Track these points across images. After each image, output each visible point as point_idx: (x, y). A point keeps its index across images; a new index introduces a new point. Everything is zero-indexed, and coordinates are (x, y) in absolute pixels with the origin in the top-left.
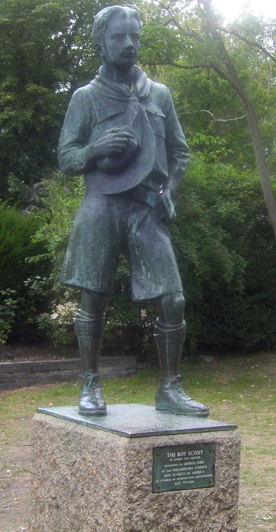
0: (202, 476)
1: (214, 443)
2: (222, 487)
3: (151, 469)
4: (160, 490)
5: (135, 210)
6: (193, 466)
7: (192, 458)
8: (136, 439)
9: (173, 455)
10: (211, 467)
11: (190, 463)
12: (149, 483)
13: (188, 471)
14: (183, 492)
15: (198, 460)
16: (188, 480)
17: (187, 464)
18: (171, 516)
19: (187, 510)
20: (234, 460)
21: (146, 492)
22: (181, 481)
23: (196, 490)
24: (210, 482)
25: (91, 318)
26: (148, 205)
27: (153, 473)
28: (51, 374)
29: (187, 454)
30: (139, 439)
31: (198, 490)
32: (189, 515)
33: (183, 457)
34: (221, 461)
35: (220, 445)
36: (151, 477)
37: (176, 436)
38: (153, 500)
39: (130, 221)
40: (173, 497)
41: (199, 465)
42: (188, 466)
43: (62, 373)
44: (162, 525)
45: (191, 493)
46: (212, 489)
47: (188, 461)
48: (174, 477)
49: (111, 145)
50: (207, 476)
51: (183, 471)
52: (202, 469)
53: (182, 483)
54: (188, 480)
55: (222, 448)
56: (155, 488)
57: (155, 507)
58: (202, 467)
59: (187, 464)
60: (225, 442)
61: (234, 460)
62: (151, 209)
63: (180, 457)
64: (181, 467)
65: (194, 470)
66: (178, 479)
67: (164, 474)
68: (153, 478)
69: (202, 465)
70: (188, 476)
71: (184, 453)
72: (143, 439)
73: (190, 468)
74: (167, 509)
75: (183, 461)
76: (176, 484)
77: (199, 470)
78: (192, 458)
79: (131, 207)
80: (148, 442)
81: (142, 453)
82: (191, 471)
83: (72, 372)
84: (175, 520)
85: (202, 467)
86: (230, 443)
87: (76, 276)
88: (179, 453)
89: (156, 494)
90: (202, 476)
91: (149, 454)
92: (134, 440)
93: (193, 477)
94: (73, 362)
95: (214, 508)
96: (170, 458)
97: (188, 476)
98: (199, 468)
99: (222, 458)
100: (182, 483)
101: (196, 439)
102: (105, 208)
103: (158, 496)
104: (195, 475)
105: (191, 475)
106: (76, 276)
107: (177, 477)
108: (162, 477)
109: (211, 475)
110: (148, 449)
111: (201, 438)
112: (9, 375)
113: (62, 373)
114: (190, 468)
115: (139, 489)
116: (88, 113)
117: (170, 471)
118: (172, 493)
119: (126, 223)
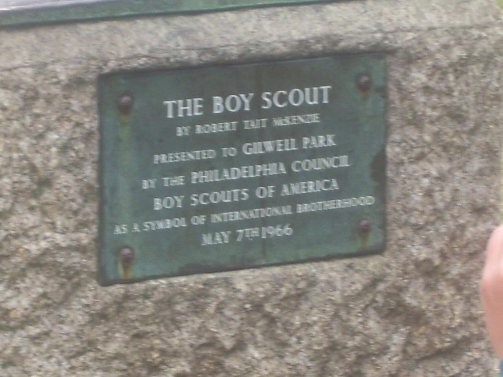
0: (330, 205)
3: (89, 172)
4: (136, 271)
6: (285, 158)
7: (278, 122)
9: (193, 107)
11: (269, 146)
12: (85, 237)
13: (264, 181)
14: (242, 280)
16: (264, 222)
22: (231, 227)
23: (299, 270)
24: (364, 231)
27: (100, 194)
29: (257, 102)
31: (311, 268)
33: (241, 116)
36: (90, 210)
37: (203, 19)
40: (197, 301)
41: (314, 153)
42: (263, 159)
45: (278, 282)
47: (261, 135)
48: (200, 210)
50: (349, 203)
51: (241, 183)
52: (327, 174)
53: (234, 236)
54: (264, 222)
56: (112, 261)
58: (328, 163)
59: (255, 149)
63: (226, 116)
64: (230, 162)
65: (290, 177)
66: (216, 218)
67: (151, 195)
68: (101, 214)
69: (325, 152)
70: (264, 203)
71: (244, 101)
73: (272, 169)
75: (240, 137)
76: (207, 240)
77: (313, 175)
78: (278, 122)
82: (278, 181)
85: (328, 163)
88: (217, 101)
89: (118, 289)
90: (330, 205)
93: (286, 211)
96: (178, 121)
97: (264, 203)
98: (316, 165)
100: (234, 236)
101: (297, 35)
103: (127, 297)
104: (294, 200)
105: (277, 200)
108: (143, 208)
109: (367, 200)
111: (320, 29)
114: (272, 169)
117: (179, 181)
118: (192, 282)
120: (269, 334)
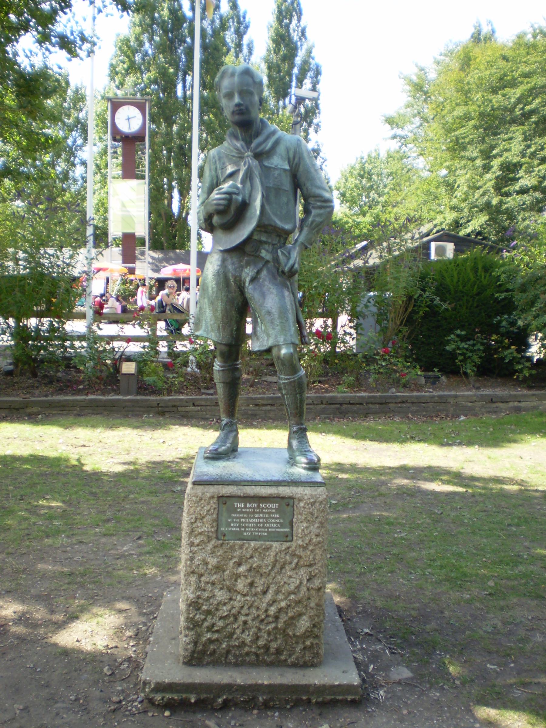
0: (277, 530)
1: (291, 498)
2: (300, 542)
3: (215, 516)
4: (226, 538)
5: (248, 264)
6: (266, 519)
7: (264, 511)
8: (200, 487)
9: (242, 505)
10: (288, 522)
11: (261, 515)
12: (213, 530)
13: (259, 523)
14: (253, 544)
15: (273, 513)
16: (260, 531)
17: (258, 516)
18: (239, 564)
19: (256, 562)
20: (317, 518)
21: (209, 539)
22: (251, 532)
23: (268, 543)
24: (287, 536)
25: (221, 367)
26: (262, 258)
27: (217, 520)
28: (511, 404)
29: (258, 506)
30: (202, 487)
31: (272, 543)
32: (259, 567)
33: (254, 508)
34: (300, 517)
35: (300, 500)
36: (215, 524)
37: (246, 487)
38: (217, 547)
39: (244, 275)
40: (241, 547)
41: (273, 518)
42: (259, 518)
43: (523, 404)
44: (228, 572)
45: (262, 545)
46: (288, 544)
47: (259, 513)
48: (243, 527)
49: (215, 202)
50: (283, 530)
51: (254, 523)
52: (277, 523)
53: (252, 534)
54: (260, 531)
55: (302, 504)
56: (218, 535)
57: (219, 554)
58: (278, 521)
59: (258, 516)
60: (306, 498)
61: (317, 518)
62: (267, 262)
63: (250, 508)
64: (251, 518)
65: (267, 523)
66: (247, 529)
67: (230, 523)
68: (218, 525)
69: (276, 518)
70: (260, 527)
71: (256, 505)
72: (207, 487)
73: (262, 520)
74: (233, 557)
75: (254, 512)
76: (245, 534)
77: (273, 523)
78: (264, 511)
79: (244, 261)
80: (212, 490)
81: (205, 500)
82: (264, 523)
83: (532, 404)
84: (242, 569)
85: (278, 521)
86: (312, 500)
87: (203, 327)
88: (248, 505)
89: (221, 542)
90: (277, 530)
91: (215, 500)
92: (196, 487)
93: (266, 530)
94: (533, 395)
95: (290, 563)
96: (237, 508)
97: (260, 527)
98: (273, 521)
99: (301, 514)
100: (252, 534)
101: (269, 492)
102: (219, 263)
103: (223, 543)
104: (268, 528)
105: (263, 527)
106: (203, 327)
107: (245, 527)
108: (228, 525)
109: (288, 530)
110: (212, 497)
111: (276, 492)
112: (469, 404)
113: (523, 404)
114: (262, 520)
115: (201, 534)
116: (213, 173)
117: (238, 520)
118: (240, 542)
119: (240, 277)
120: (260, 555)
